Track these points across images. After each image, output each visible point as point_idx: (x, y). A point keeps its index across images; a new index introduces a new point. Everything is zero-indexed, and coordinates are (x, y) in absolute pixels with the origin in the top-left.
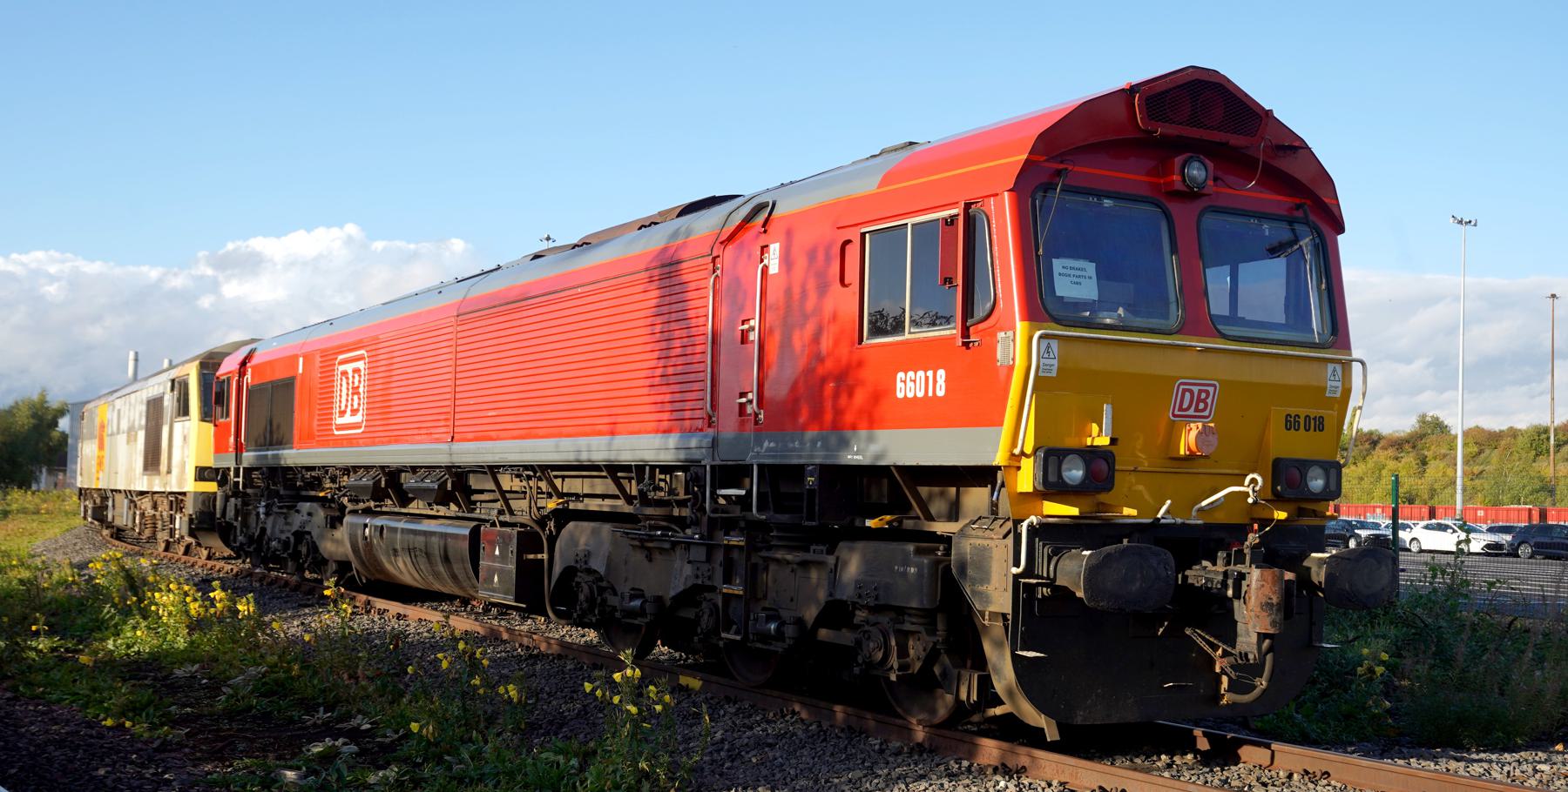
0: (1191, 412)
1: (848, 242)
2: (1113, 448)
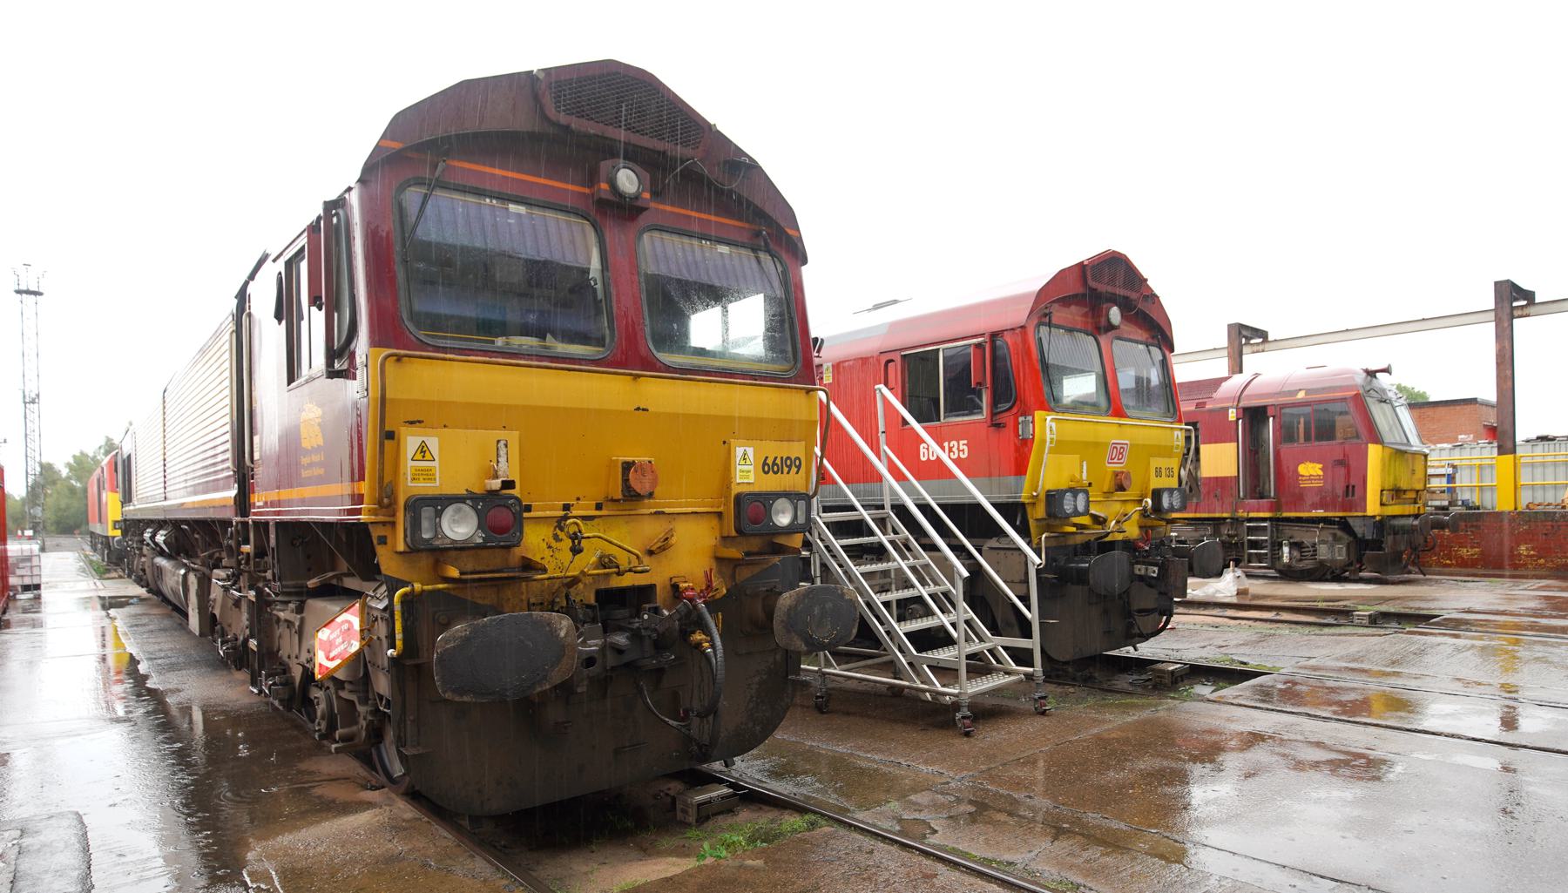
0: (1115, 460)
1: (892, 361)
2: (1088, 489)
